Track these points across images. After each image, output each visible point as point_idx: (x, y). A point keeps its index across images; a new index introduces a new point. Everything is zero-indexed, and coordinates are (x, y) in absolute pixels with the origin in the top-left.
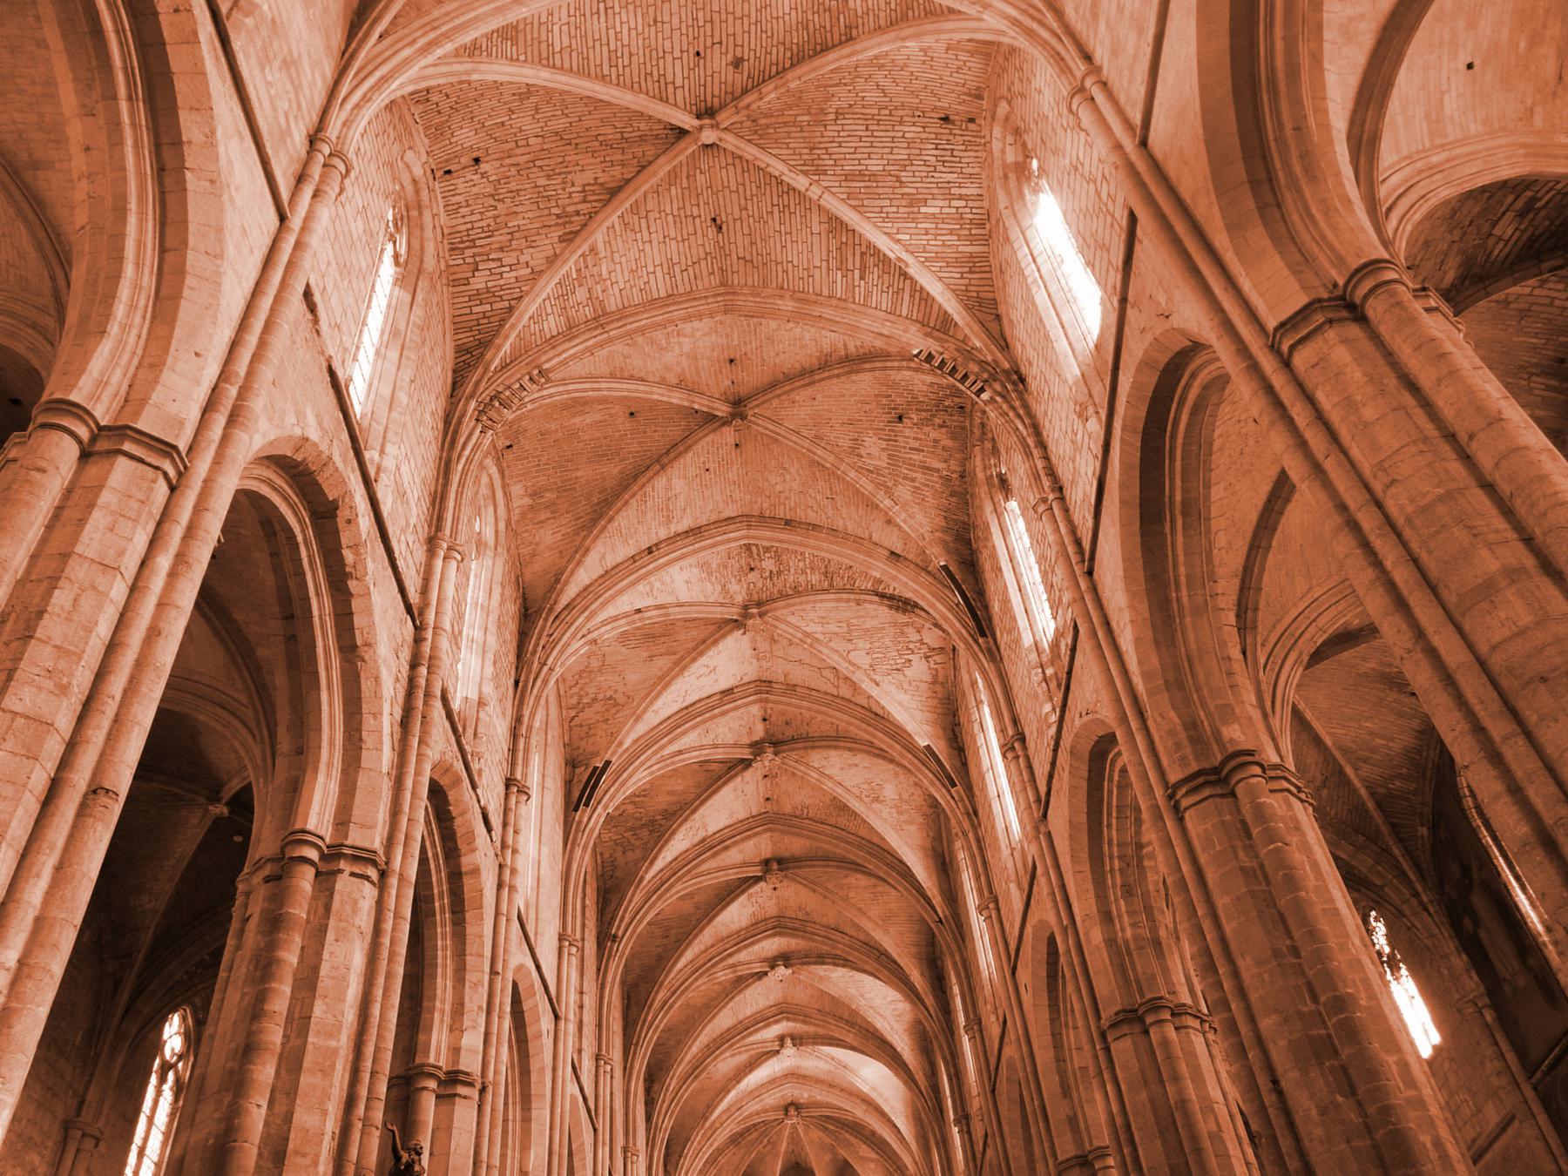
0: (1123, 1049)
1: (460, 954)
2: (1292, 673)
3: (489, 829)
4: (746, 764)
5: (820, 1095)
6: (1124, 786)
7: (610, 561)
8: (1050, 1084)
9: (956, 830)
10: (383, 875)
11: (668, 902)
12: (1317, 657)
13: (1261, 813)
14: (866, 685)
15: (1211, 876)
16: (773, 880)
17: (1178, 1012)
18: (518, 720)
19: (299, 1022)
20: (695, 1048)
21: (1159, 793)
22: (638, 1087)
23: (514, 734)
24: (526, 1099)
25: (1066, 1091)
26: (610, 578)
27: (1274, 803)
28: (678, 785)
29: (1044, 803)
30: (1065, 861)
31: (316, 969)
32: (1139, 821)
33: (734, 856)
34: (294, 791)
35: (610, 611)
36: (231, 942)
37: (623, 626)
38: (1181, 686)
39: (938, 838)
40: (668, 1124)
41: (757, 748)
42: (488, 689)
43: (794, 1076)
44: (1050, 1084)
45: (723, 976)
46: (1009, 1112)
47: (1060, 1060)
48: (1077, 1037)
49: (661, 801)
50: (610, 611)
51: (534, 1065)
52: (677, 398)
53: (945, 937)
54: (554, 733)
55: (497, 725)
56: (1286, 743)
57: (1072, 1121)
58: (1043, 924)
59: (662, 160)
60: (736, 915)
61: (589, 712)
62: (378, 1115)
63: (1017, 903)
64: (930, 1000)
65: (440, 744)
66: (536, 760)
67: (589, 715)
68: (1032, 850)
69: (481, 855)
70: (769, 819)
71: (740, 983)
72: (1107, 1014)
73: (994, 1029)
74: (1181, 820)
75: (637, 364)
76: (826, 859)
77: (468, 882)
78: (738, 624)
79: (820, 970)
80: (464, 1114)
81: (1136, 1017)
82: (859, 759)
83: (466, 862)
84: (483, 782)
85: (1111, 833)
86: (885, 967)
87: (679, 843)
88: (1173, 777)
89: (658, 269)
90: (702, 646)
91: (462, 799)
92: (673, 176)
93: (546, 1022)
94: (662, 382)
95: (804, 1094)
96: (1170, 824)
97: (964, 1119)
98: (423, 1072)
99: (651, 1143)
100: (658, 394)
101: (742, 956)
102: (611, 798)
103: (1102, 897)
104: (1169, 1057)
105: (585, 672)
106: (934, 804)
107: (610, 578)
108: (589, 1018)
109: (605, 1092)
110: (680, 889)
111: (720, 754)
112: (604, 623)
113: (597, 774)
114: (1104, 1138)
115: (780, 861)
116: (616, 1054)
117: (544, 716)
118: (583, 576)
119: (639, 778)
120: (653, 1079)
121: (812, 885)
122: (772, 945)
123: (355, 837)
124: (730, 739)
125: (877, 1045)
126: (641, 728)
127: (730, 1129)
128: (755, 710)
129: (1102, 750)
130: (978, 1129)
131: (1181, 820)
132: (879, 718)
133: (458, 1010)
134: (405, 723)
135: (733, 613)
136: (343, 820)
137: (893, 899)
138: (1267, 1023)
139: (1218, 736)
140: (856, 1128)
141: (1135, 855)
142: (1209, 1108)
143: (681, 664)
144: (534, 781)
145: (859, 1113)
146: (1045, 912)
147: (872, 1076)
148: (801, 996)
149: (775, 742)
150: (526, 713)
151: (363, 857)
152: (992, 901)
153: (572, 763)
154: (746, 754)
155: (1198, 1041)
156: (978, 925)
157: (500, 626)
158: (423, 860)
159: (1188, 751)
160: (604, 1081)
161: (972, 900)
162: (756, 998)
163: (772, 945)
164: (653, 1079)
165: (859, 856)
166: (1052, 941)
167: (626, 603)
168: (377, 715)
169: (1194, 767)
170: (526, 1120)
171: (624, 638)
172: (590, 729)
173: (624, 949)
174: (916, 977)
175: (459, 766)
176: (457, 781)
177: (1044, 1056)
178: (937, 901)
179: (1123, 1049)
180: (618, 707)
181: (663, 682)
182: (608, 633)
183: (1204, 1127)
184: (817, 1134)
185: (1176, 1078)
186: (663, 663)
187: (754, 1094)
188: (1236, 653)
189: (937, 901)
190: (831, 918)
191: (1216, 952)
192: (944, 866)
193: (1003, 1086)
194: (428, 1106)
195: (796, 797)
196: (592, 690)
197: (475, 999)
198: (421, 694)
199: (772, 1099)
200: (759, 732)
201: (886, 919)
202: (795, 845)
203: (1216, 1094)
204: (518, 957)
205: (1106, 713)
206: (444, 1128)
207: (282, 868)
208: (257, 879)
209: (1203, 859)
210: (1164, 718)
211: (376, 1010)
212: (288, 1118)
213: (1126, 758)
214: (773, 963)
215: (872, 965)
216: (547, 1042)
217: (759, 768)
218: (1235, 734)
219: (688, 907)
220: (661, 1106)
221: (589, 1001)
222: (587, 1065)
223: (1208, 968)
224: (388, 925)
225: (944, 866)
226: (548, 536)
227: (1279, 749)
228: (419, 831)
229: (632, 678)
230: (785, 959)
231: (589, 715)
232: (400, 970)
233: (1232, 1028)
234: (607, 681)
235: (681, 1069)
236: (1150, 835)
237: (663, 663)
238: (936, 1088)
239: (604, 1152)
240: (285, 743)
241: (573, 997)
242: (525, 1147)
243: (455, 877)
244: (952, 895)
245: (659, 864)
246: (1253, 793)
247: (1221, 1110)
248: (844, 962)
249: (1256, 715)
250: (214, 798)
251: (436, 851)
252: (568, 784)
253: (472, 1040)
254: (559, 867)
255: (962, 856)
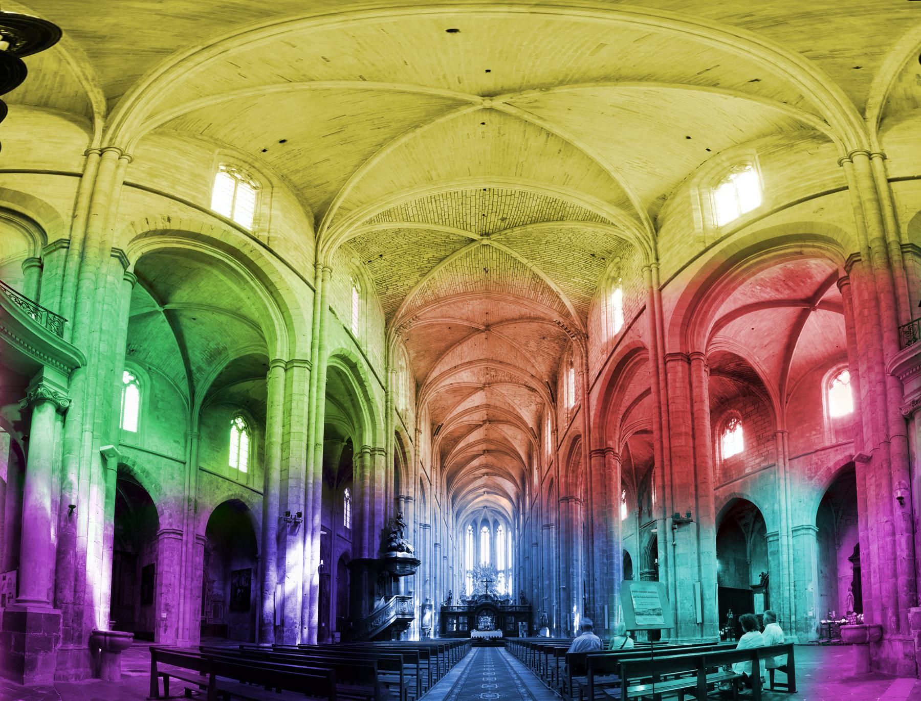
0: (562, 505)
1: (407, 471)
2: (629, 435)
3: (412, 441)
4: (481, 426)
5: (492, 505)
6: (580, 448)
7: (443, 370)
8: (544, 510)
9: (535, 449)
10: (386, 454)
11: (459, 458)
12: (636, 433)
13: (610, 463)
14: (518, 409)
15: (593, 473)
16: (486, 455)
17: (577, 500)
18: (417, 414)
19: (372, 488)
20: (464, 493)
21: (587, 452)
22: (450, 501)
23: (416, 418)
24: (425, 502)
25: (547, 511)
26: (443, 375)
27: (613, 461)
28: (462, 430)
29: (558, 447)
30: (560, 462)
31: (374, 476)
32: (581, 457)
33: (476, 448)
34: (361, 436)
35: (443, 384)
36: (354, 472)
37: (447, 388)
38: (602, 428)
39: (530, 450)
40: (457, 509)
41: (484, 422)
42: (408, 406)
43: (487, 501)
44: (544, 510)
45: (471, 477)
46: (534, 514)
47: (548, 505)
48: (553, 501)
49: (457, 434)
50: (443, 384)
51: (426, 495)
52: (466, 324)
53: (527, 474)
54: (427, 416)
55: (411, 415)
56: (621, 449)
57: (548, 518)
58: (551, 475)
59: (463, 249)
60: (475, 463)
61: (437, 411)
62: (392, 506)
63: (546, 470)
64: (521, 487)
65: (396, 421)
66: (423, 424)
67: (437, 412)
68: (553, 457)
69: (410, 448)
70: (486, 440)
71: (475, 479)
72: (561, 497)
73: (534, 496)
74: (590, 459)
75: (451, 313)
76: (500, 451)
77: (407, 454)
78: (482, 389)
79: (496, 477)
80: (411, 505)
81: (567, 499)
82: (512, 427)
83: (406, 450)
84: (409, 430)
85: (573, 458)
86: (511, 478)
87: (462, 444)
88: (592, 449)
89: (461, 285)
90: (470, 394)
91: (404, 434)
92: (468, 255)
93: (428, 486)
94: (461, 318)
95: (488, 504)
96: (588, 459)
97: (524, 514)
98: (401, 497)
99: (453, 512)
100: (459, 322)
101: (476, 472)
102: (444, 433)
103: (567, 472)
104: (572, 509)
105: (435, 401)
106: (530, 442)
107: (443, 375)
108: (439, 485)
109: (442, 501)
110: (461, 456)
111: (474, 423)
112: (441, 387)
113: (440, 427)
114: (553, 522)
115: (488, 451)
116: (445, 490)
117: (424, 412)
118: (434, 374)
119: (451, 428)
120: (454, 498)
121: (495, 457)
122: (484, 470)
123: (378, 446)
124: (477, 419)
125: (507, 496)
126: (452, 415)
127: (471, 510)
128: (485, 412)
129: (577, 438)
130: (527, 516)
131: (590, 459)
132: (520, 418)
133: (408, 483)
134: (386, 417)
135: (481, 386)
136: (374, 442)
137: (516, 463)
138: (594, 506)
139: (606, 442)
140: (500, 513)
141: (577, 464)
142: (577, 520)
143: (464, 398)
144: (423, 429)
145: (501, 510)
146: (552, 472)
147: (505, 503)
148: (490, 483)
149: (490, 421)
150: (419, 412)
151: (381, 450)
152: (540, 467)
153: (433, 424)
154: (481, 423)
155: (579, 507)
156: (536, 473)
157: (410, 389)
158: (396, 450)
159: (598, 444)
160: (442, 499)
161: (535, 466)
162: (479, 482)
163: (484, 470)
164: (454, 498)
165: (509, 452)
166: (552, 479)
167: (448, 382)
168: (379, 416)
169: (598, 448)
170: (425, 507)
171: (447, 391)
172: (438, 416)
173: (447, 469)
174: (518, 482)
175: (402, 426)
176: (402, 430)
177: (544, 503)
178: (527, 465)
179: (562, 505)
180: (445, 410)
181: (459, 403)
182: (442, 390)
183: (575, 523)
184: (490, 513)
185: (572, 513)
186: (459, 398)
187: (478, 503)
188: (618, 425)
189: (527, 465)
190: (499, 466)
191: (589, 489)
192: (530, 457)
193: (534, 508)
194: (403, 504)
195: (494, 435)
196: (438, 405)
197: (412, 481)
198: (389, 409)
199: (481, 505)
200: (485, 418)
201: (513, 468)
202: (492, 447)
203: (579, 518)
204: (421, 471)
205: (581, 430)
206: (407, 509)
207: (362, 455)
208: (357, 458)
209: (593, 469)
210: (595, 435)
211: (389, 484)
212: (374, 507)
213: (582, 441)
214: (484, 474)
215: (508, 478)
216: (429, 490)
217: (484, 427)
218: (610, 443)
219: (463, 460)
220: (456, 504)
221: (439, 481)
222: (438, 495)
223: (586, 492)
224: (389, 465)
225: (530, 457)
226: (423, 364)
227: (619, 450)
228: (394, 443)
229: (449, 402)
230: (487, 474)
231: (437, 412)
232: (393, 475)
233: (587, 505)
234: (442, 403)
235: (460, 497)
236: (582, 460)
237: (459, 398)
238: (519, 507)
239: (442, 514)
240: (356, 426)
241: (435, 480)
242: (425, 512)
243: (404, 453)
244: (531, 464)
245: (456, 449)
246: (610, 458)
247: (579, 521)
248: (502, 476)
249: (617, 441)
250: (343, 441)
251: (398, 447)
252: (432, 430)
253: (411, 490)
254: (430, 450)
255: (535, 455)
